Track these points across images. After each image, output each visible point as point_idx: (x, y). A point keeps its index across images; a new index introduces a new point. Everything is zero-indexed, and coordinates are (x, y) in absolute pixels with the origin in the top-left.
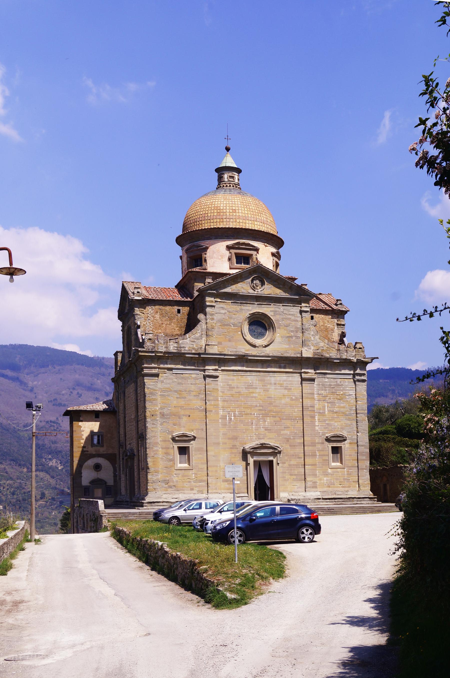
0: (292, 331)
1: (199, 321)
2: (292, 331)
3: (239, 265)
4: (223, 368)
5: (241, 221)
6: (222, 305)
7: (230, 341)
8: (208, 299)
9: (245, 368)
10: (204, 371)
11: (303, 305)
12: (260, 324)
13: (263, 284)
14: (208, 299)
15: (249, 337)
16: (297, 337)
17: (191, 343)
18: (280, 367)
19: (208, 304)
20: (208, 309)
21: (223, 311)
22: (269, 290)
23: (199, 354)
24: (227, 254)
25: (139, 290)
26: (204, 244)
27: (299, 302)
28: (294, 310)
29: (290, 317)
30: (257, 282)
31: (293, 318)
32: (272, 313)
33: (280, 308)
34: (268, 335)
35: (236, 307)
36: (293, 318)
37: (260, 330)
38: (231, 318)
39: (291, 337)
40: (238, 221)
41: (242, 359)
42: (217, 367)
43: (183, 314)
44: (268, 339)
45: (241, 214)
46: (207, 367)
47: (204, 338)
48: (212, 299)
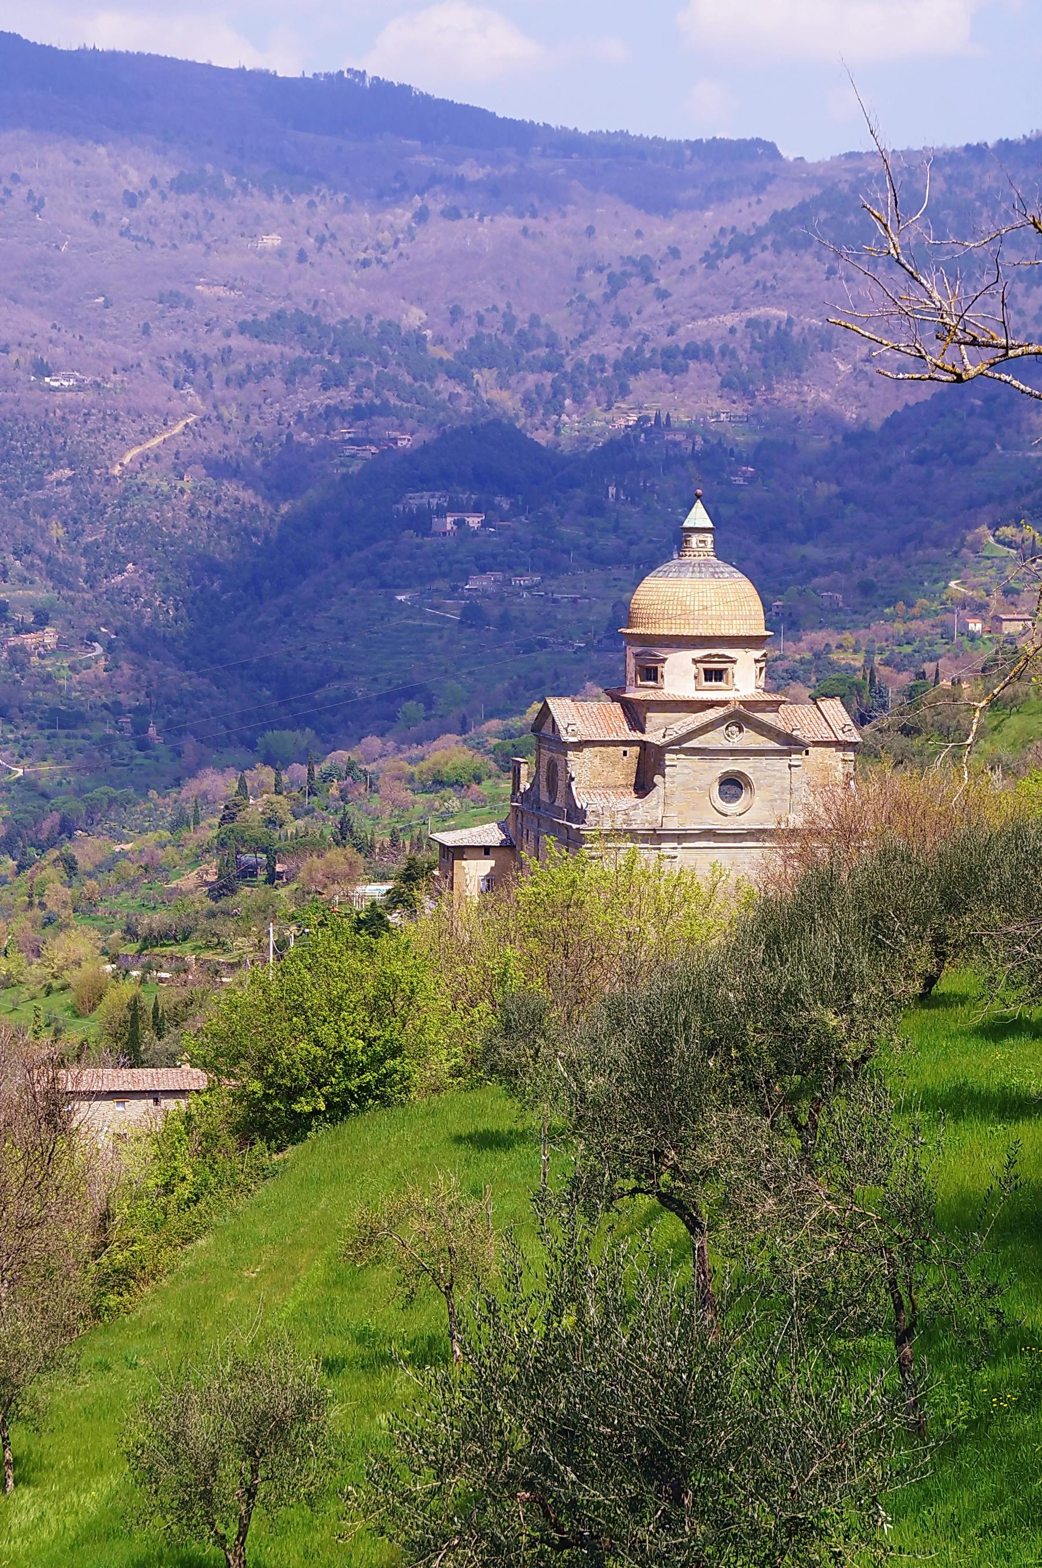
0: (776, 793)
1: (655, 785)
2: (776, 793)
3: (709, 683)
4: (685, 845)
5: (714, 622)
6: (685, 763)
7: (693, 809)
8: (668, 756)
9: (712, 844)
10: (659, 849)
11: (793, 756)
12: (733, 785)
13: (741, 730)
14: (668, 756)
15: (720, 803)
16: (783, 800)
17: (645, 813)
18: (758, 841)
19: (667, 763)
20: (667, 770)
21: (687, 771)
22: (749, 739)
23: (654, 830)
24: (693, 669)
25: (574, 727)
26: (661, 653)
27: (789, 753)
28: (783, 763)
29: (775, 773)
30: (734, 729)
31: (779, 775)
32: (751, 770)
33: (763, 762)
34: (745, 795)
35: (706, 765)
36: (779, 775)
37: (734, 790)
38: (695, 779)
39: (775, 800)
40: (710, 622)
41: (709, 834)
42: (675, 845)
43: (631, 756)
44: (744, 804)
45: (714, 613)
46: (663, 845)
47: (661, 808)
48: (673, 756)
